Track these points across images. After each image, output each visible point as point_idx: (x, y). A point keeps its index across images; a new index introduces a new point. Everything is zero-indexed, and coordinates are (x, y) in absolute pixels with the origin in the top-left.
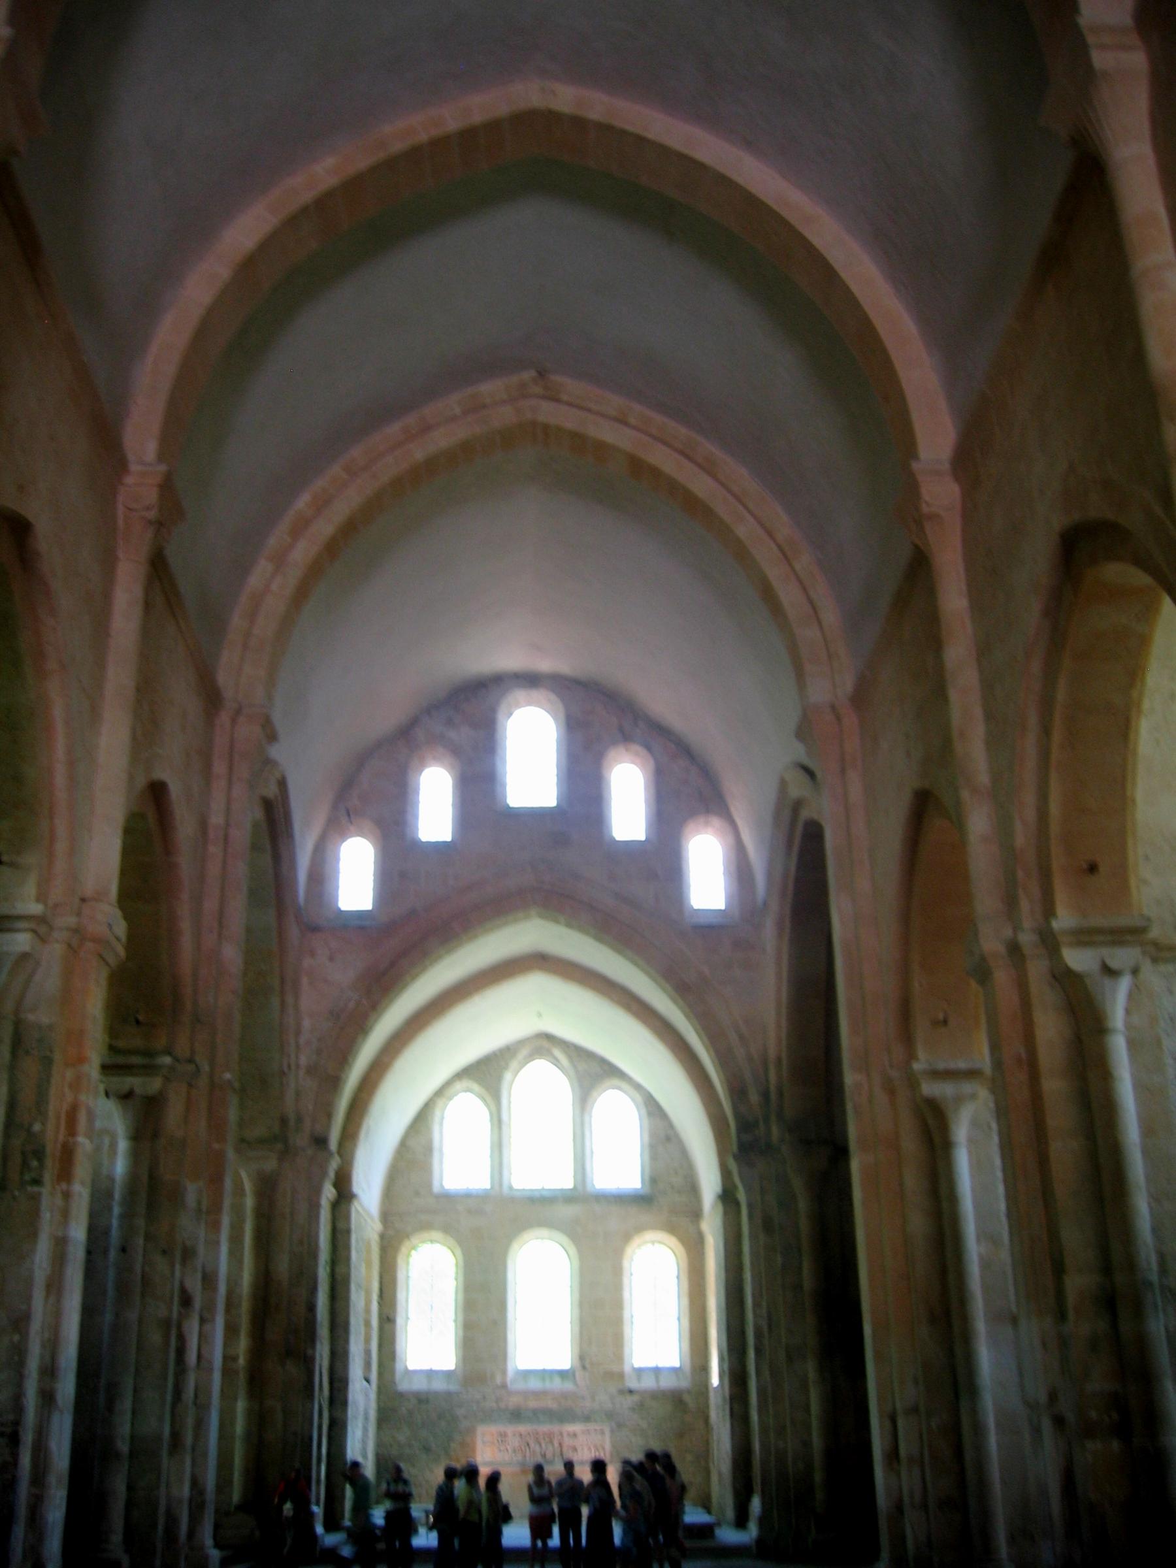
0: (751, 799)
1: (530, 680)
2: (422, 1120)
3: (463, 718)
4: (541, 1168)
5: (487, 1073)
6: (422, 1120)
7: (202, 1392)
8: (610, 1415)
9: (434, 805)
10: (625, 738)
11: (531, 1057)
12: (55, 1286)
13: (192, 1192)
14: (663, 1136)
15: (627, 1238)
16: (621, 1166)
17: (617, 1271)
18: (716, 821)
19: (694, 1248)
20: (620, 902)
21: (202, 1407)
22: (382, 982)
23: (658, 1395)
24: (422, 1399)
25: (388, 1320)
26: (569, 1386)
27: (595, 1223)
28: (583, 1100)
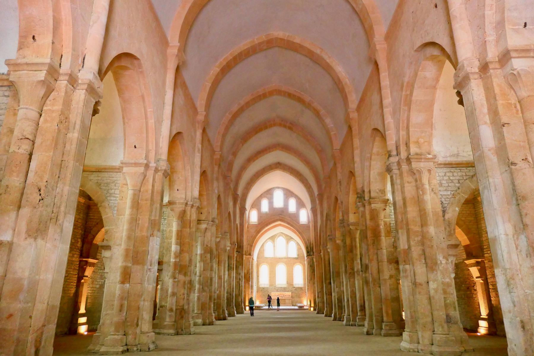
0: (309, 205)
1: (278, 188)
2: (263, 246)
3: (268, 193)
4: (281, 253)
5: (273, 238)
6: (263, 245)
7: (242, 289)
8: (291, 291)
9: (265, 206)
10: (292, 197)
11: (279, 236)
12: (233, 280)
13: (240, 267)
14: (299, 249)
15: (294, 264)
16: (293, 252)
17: (293, 269)
18: (305, 209)
19: (304, 265)
20: (291, 221)
21: (242, 291)
22: (258, 232)
23: (298, 288)
24: (263, 288)
25: (258, 276)
26: (285, 286)
27: (290, 262)
28: (288, 242)
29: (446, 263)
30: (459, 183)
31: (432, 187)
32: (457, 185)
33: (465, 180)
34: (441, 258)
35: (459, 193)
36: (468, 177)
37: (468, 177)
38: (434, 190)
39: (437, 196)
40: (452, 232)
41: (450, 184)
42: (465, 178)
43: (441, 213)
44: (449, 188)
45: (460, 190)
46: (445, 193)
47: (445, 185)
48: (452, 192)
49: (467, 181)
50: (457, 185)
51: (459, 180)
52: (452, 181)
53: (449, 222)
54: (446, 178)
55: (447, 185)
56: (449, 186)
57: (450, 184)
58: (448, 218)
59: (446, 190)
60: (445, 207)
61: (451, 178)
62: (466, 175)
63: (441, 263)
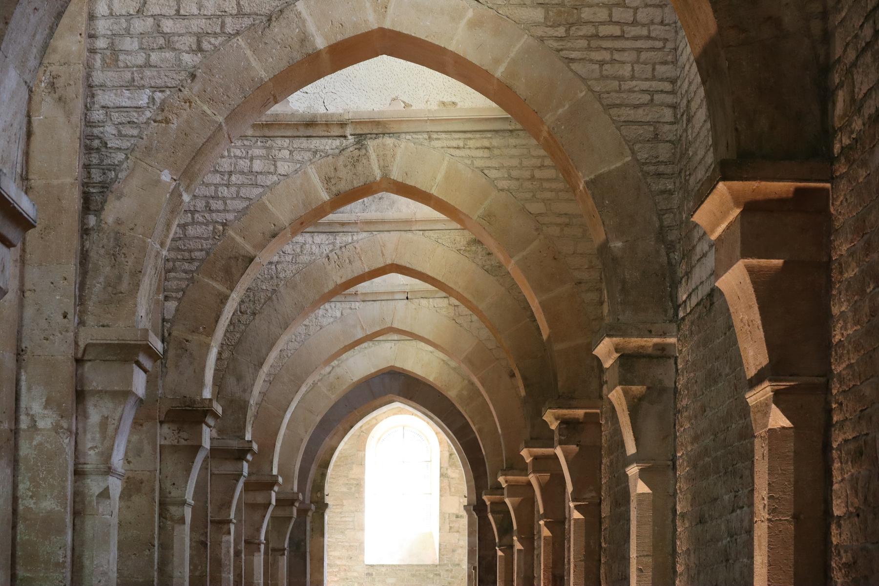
29: (56, 428)
30: (200, 49)
31: (54, 69)
32: (188, 59)
33: (230, 36)
34: (37, 408)
35: (188, 101)
36: (247, 21)
37: (247, 21)
38: (60, 83)
39: (68, 114)
40: (124, 286)
41: (154, 57)
42: (229, 29)
43: (73, 200)
44: (148, 73)
45: (197, 86)
46: (125, 99)
47: (130, 60)
48: (158, 96)
49: (241, 41)
50: (188, 59)
51: (199, 37)
52: (169, 45)
53: (118, 237)
54: (140, 25)
55: (140, 59)
56: (148, 65)
57: (154, 57)
58: (119, 222)
59: (131, 85)
60: (114, 167)
61: (168, 26)
62: (240, 14)
63: (33, 426)
